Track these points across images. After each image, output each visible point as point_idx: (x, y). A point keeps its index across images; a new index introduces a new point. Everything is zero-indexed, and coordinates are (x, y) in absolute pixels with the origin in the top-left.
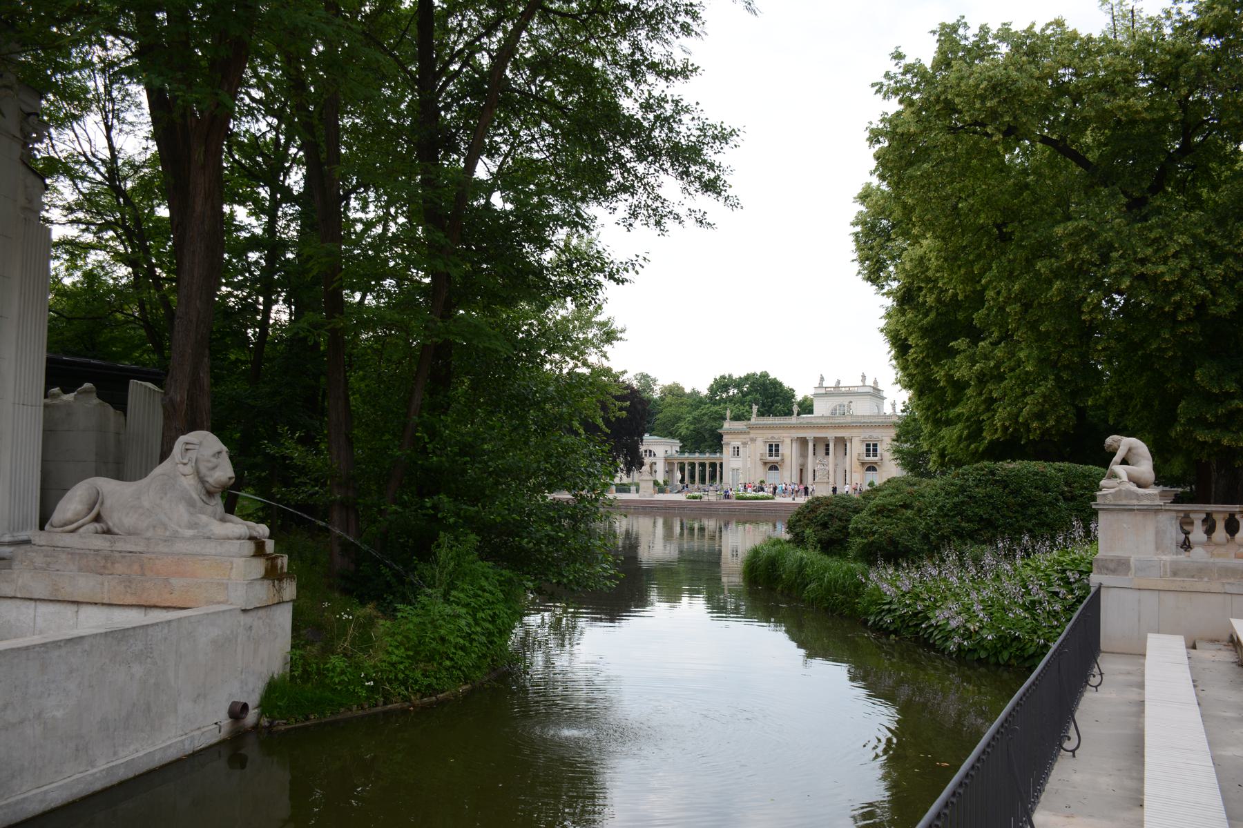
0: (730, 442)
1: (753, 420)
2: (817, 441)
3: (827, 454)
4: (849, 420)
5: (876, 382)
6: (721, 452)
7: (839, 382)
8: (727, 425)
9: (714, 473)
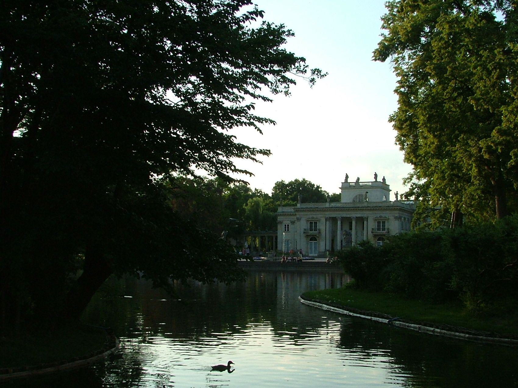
2: (343, 219)
4: (366, 204)
5: (384, 179)
7: (358, 179)
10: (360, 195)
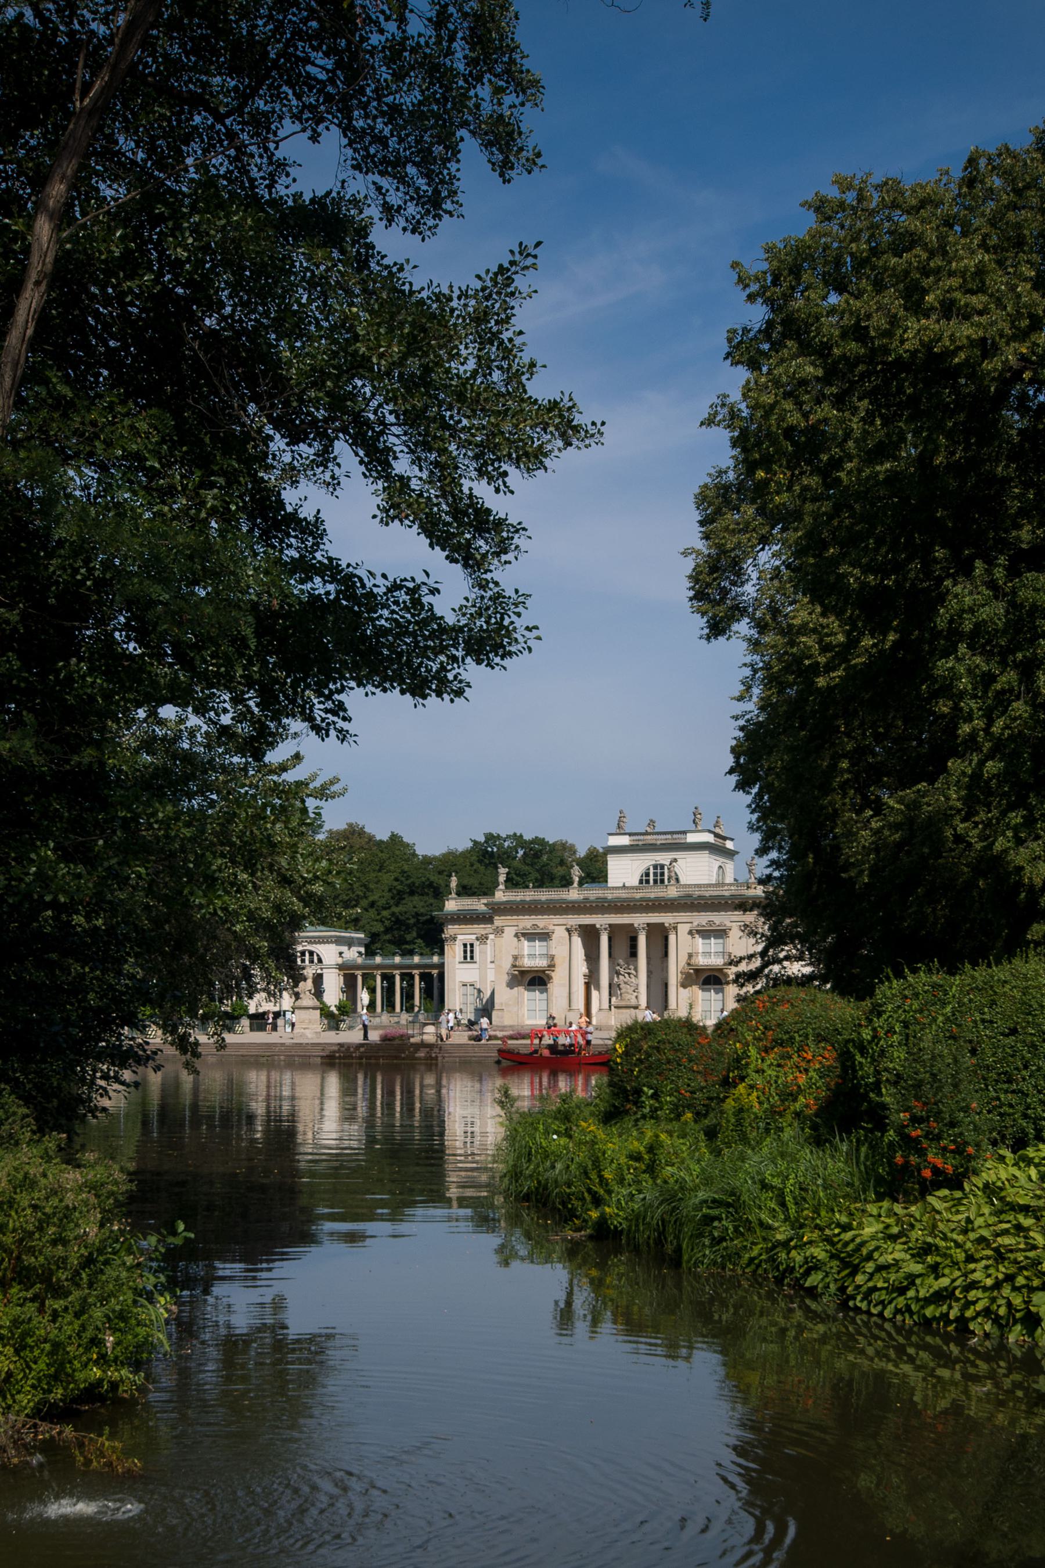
0: (460, 935)
1: (501, 895)
2: (613, 929)
3: (634, 954)
4: (672, 892)
6: (442, 953)
8: (452, 905)
9: (434, 989)
10: (655, 867)
